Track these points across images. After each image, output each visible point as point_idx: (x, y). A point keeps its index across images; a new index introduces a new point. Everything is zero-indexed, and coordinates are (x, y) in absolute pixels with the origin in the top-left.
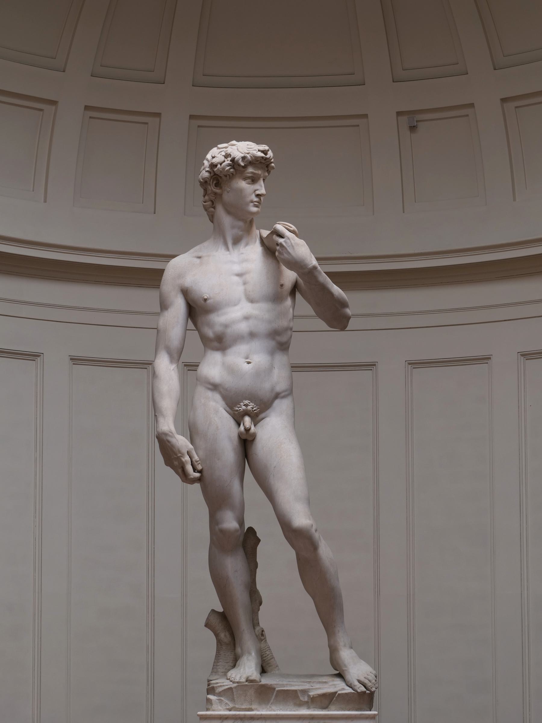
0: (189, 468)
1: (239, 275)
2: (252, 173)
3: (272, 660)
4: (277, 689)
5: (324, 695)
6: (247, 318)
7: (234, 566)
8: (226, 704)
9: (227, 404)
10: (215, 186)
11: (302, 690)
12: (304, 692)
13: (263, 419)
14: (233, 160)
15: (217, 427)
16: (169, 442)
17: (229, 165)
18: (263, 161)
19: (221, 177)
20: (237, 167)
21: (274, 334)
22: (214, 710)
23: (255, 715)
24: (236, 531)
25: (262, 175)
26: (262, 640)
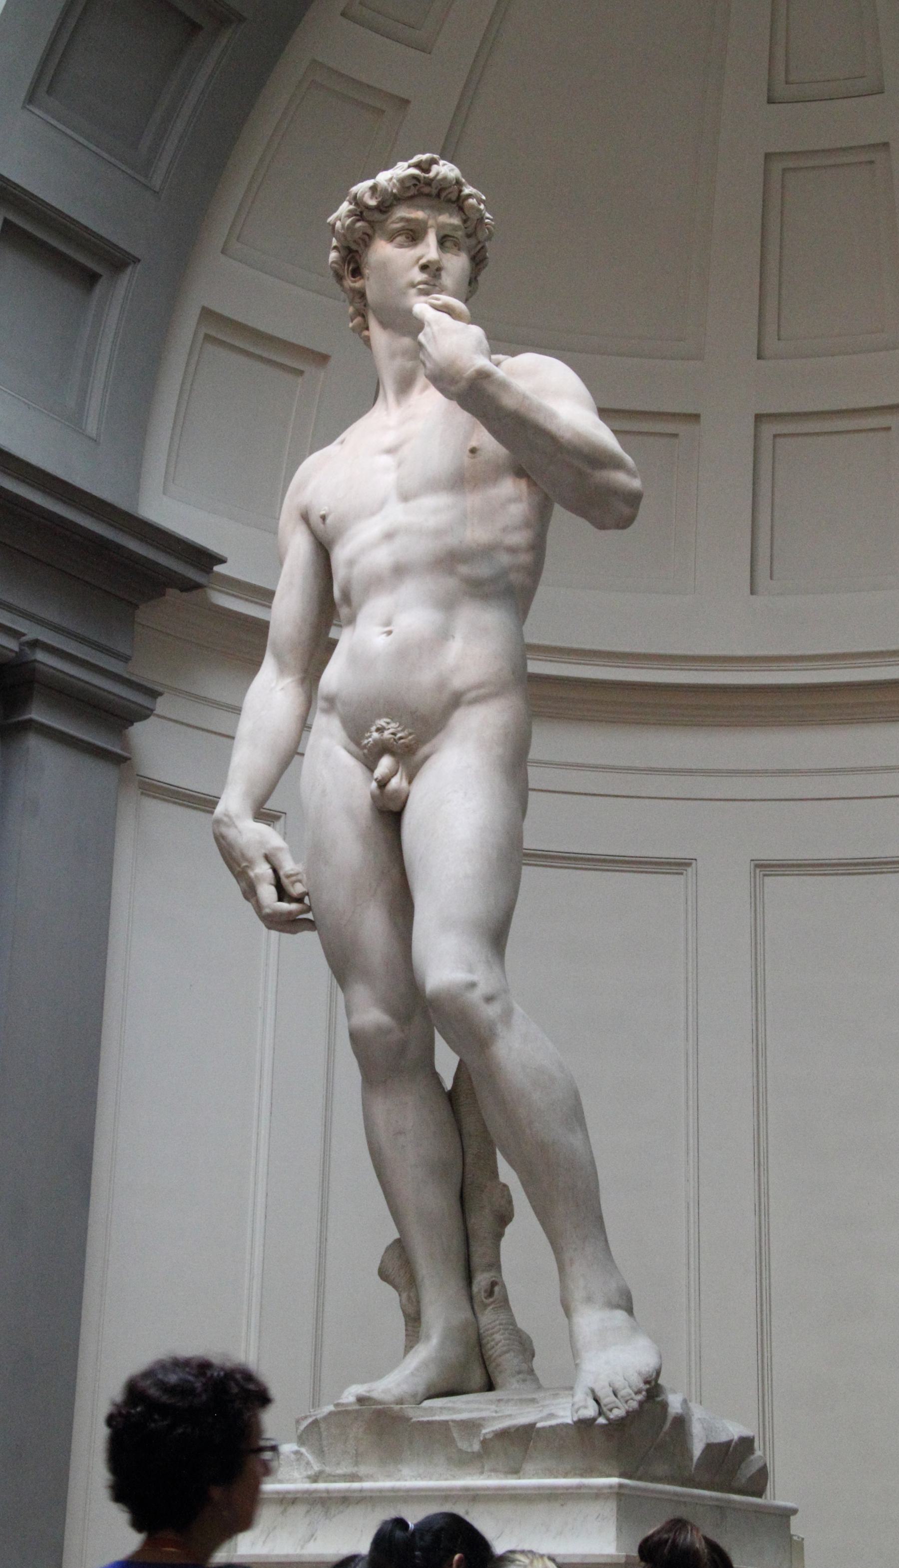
0: (267, 893)
1: (391, 451)
2: (402, 219)
3: (507, 1355)
4: (414, 1420)
5: (503, 1434)
6: (389, 536)
7: (410, 1121)
8: (308, 1463)
9: (350, 737)
10: (354, 276)
11: (462, 1421)
12: (470, 1427)
13: (426, 758)
14: (356, 200)
15: (324, 791)
16: (223, 837)
17: (351, 213)
18: (426, 190)
19: (357, 251)
20: (373, 218)
21: (449, 560)
22: (280, 1482)
23: (348, 1490)
24: (381, 1030)
25: (431, 222)
26: (486, 1306)
